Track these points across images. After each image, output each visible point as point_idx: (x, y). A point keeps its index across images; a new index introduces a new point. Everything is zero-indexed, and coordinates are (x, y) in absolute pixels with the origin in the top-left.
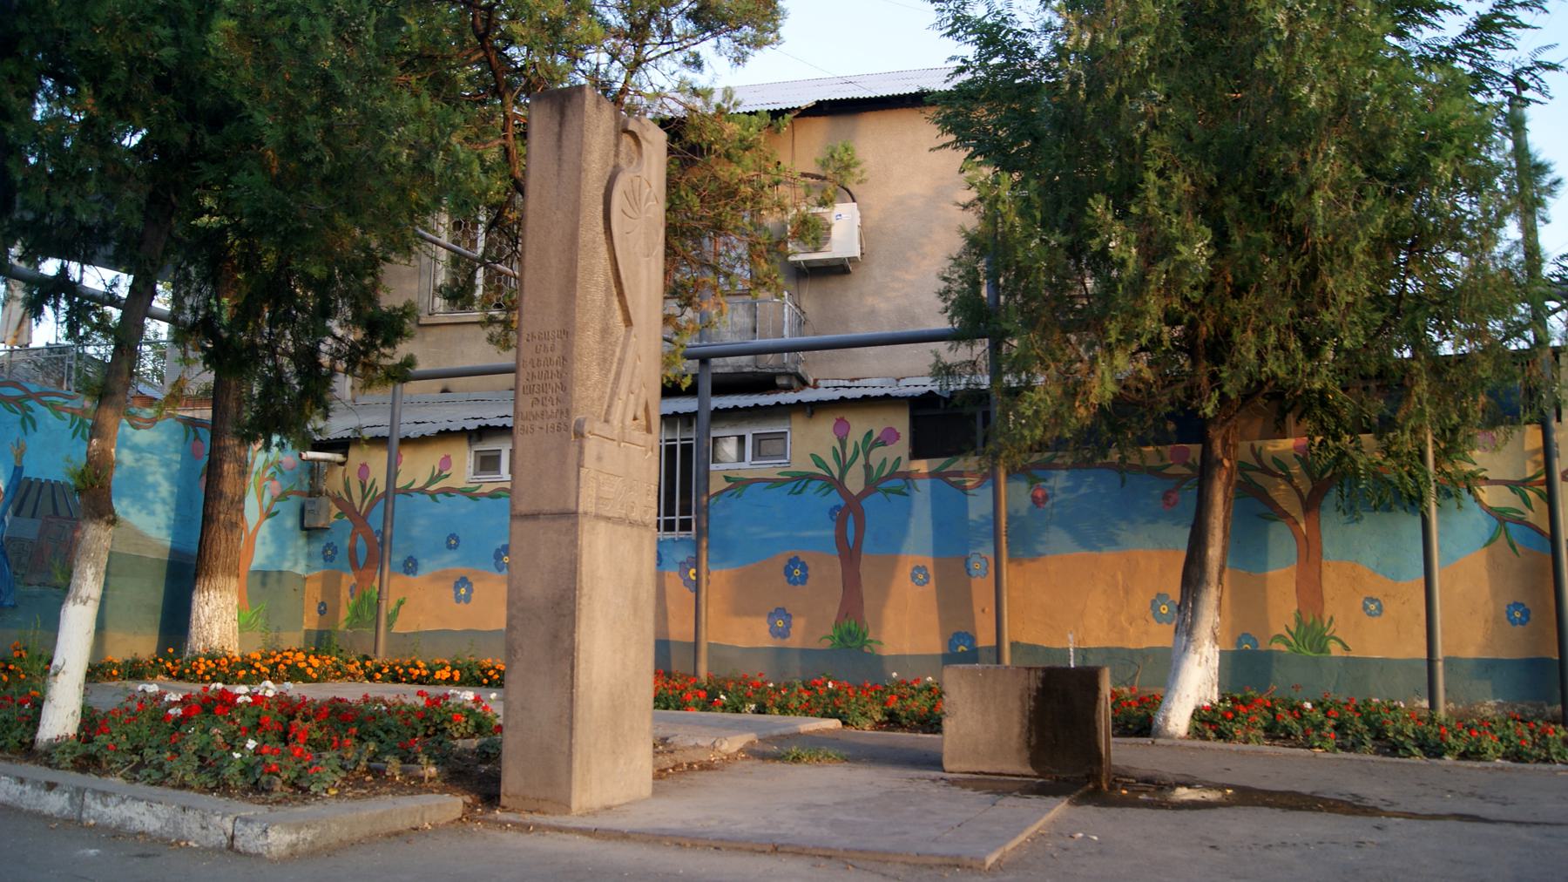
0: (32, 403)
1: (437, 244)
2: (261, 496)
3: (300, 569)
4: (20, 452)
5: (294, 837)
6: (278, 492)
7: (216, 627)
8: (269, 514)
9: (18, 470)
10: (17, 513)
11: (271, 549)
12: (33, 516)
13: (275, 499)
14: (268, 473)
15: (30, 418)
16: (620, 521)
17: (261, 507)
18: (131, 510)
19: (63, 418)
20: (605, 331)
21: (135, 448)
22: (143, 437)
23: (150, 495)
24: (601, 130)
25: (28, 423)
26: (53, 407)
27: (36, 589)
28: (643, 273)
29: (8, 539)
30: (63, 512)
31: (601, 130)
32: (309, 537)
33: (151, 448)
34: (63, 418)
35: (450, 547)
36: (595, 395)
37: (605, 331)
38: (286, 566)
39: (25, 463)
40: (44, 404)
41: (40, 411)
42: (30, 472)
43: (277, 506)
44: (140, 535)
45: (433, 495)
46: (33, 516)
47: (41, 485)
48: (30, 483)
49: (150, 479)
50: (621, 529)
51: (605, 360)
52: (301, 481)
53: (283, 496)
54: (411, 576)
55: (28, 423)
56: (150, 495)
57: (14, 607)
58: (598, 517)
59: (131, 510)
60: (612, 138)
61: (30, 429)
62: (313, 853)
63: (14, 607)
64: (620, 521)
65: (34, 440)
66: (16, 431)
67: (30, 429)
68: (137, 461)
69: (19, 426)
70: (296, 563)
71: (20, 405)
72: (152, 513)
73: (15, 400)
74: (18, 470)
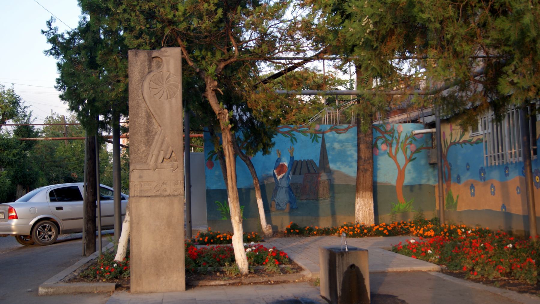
0: (294, 132)
1: (307, 60)
2: (405, 152)
3: (432, 182)
4: (292, 153)
5: (47, 290)
6: (414, 149)
7: (361, 213)
8: (411, 160)
9: (292, 158)
10: (294, 174)
11: (414, 175)
12: (300, 174)
13: (413, 153)
14: (408, 141)
15: (294, 138)
16: (156, 196)
17: (406, 158)
18: (341, 166)
19: (307, 136)
20: (148, 132)
21: (340, 142)
22: (342, 136)
23: (350, 159)
24: (139, 63)
25: (293, 140)
26: (304, 132)
27: (305, 201)
28: (167, 106)
29: (291, 184)
30: (312, 171)
31: (139, 63)
32: (434, 167)
33: (347, 140)
34: (307, 136)
35: (468, 169)
36: (143, 155)
37: (148, 132)
38: (423, 182)
39: (294, 155)
40: (299, 132)
41: (297, 134)
42: (297, 158)
43: (414, 156)
44: (347, 176)
45: (461, 144)
46: (300, 174)
47: (302, 162)
48: (297, 162)
49: (349, 153)
50: (157, 199)
51: (148, 142)
52: (427, 142)
53: (418, 151)
54: (459, 185)
55: (293, 140)
56: (350, 159)
57: (297, 208)
58: (141, 197)
59: (341, 166)
60: (147, 63)
61: (295, 142)
62: (53, 294)
63: (297, 208)
64: (156, 196)
65: (296, 146)
66: (289, 144)
67: (295, 142)
68: (342, 146)
69: (290, 142)
70: (429, 180)
71: (289, 134)
72: (351, 167)
73: (288, 132)
74: (292, 158)
